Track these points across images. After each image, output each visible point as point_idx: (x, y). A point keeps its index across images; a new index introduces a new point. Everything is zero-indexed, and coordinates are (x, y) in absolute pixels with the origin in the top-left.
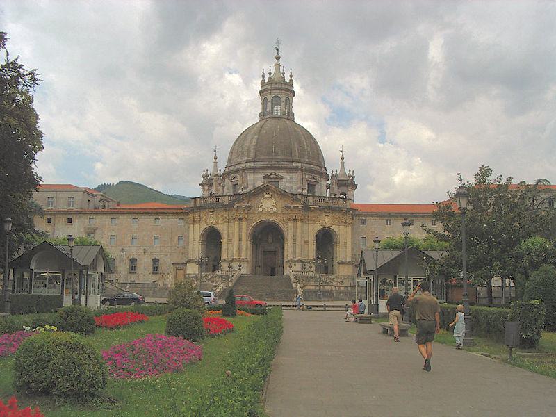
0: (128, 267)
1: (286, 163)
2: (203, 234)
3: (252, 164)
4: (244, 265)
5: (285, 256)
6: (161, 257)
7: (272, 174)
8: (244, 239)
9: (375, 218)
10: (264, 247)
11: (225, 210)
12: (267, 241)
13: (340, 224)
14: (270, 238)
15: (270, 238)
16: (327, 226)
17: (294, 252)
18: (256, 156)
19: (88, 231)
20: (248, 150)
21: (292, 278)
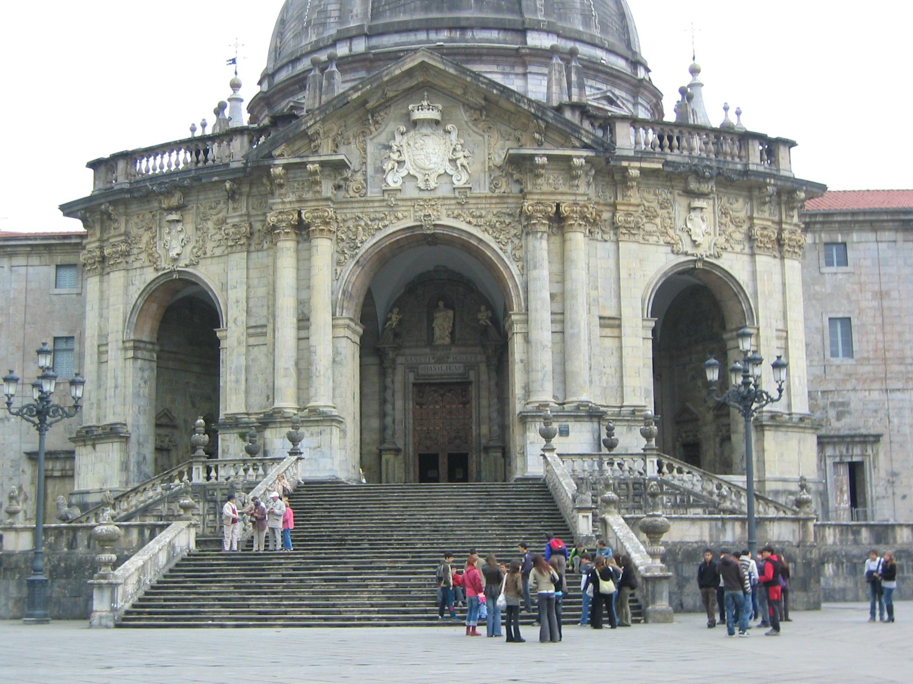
1: (494, 35)
2: (140, 311)
3: (360, 46)
5: (518, 389)
8: (322, 317)
9: (888, 235)
10: (412, 368)
11: (232, 196)
12: (430, 342)
14: (443, 323)
15: (443, 323)
16: (702, 251)
17: (563, 375)
21: (568, 487)
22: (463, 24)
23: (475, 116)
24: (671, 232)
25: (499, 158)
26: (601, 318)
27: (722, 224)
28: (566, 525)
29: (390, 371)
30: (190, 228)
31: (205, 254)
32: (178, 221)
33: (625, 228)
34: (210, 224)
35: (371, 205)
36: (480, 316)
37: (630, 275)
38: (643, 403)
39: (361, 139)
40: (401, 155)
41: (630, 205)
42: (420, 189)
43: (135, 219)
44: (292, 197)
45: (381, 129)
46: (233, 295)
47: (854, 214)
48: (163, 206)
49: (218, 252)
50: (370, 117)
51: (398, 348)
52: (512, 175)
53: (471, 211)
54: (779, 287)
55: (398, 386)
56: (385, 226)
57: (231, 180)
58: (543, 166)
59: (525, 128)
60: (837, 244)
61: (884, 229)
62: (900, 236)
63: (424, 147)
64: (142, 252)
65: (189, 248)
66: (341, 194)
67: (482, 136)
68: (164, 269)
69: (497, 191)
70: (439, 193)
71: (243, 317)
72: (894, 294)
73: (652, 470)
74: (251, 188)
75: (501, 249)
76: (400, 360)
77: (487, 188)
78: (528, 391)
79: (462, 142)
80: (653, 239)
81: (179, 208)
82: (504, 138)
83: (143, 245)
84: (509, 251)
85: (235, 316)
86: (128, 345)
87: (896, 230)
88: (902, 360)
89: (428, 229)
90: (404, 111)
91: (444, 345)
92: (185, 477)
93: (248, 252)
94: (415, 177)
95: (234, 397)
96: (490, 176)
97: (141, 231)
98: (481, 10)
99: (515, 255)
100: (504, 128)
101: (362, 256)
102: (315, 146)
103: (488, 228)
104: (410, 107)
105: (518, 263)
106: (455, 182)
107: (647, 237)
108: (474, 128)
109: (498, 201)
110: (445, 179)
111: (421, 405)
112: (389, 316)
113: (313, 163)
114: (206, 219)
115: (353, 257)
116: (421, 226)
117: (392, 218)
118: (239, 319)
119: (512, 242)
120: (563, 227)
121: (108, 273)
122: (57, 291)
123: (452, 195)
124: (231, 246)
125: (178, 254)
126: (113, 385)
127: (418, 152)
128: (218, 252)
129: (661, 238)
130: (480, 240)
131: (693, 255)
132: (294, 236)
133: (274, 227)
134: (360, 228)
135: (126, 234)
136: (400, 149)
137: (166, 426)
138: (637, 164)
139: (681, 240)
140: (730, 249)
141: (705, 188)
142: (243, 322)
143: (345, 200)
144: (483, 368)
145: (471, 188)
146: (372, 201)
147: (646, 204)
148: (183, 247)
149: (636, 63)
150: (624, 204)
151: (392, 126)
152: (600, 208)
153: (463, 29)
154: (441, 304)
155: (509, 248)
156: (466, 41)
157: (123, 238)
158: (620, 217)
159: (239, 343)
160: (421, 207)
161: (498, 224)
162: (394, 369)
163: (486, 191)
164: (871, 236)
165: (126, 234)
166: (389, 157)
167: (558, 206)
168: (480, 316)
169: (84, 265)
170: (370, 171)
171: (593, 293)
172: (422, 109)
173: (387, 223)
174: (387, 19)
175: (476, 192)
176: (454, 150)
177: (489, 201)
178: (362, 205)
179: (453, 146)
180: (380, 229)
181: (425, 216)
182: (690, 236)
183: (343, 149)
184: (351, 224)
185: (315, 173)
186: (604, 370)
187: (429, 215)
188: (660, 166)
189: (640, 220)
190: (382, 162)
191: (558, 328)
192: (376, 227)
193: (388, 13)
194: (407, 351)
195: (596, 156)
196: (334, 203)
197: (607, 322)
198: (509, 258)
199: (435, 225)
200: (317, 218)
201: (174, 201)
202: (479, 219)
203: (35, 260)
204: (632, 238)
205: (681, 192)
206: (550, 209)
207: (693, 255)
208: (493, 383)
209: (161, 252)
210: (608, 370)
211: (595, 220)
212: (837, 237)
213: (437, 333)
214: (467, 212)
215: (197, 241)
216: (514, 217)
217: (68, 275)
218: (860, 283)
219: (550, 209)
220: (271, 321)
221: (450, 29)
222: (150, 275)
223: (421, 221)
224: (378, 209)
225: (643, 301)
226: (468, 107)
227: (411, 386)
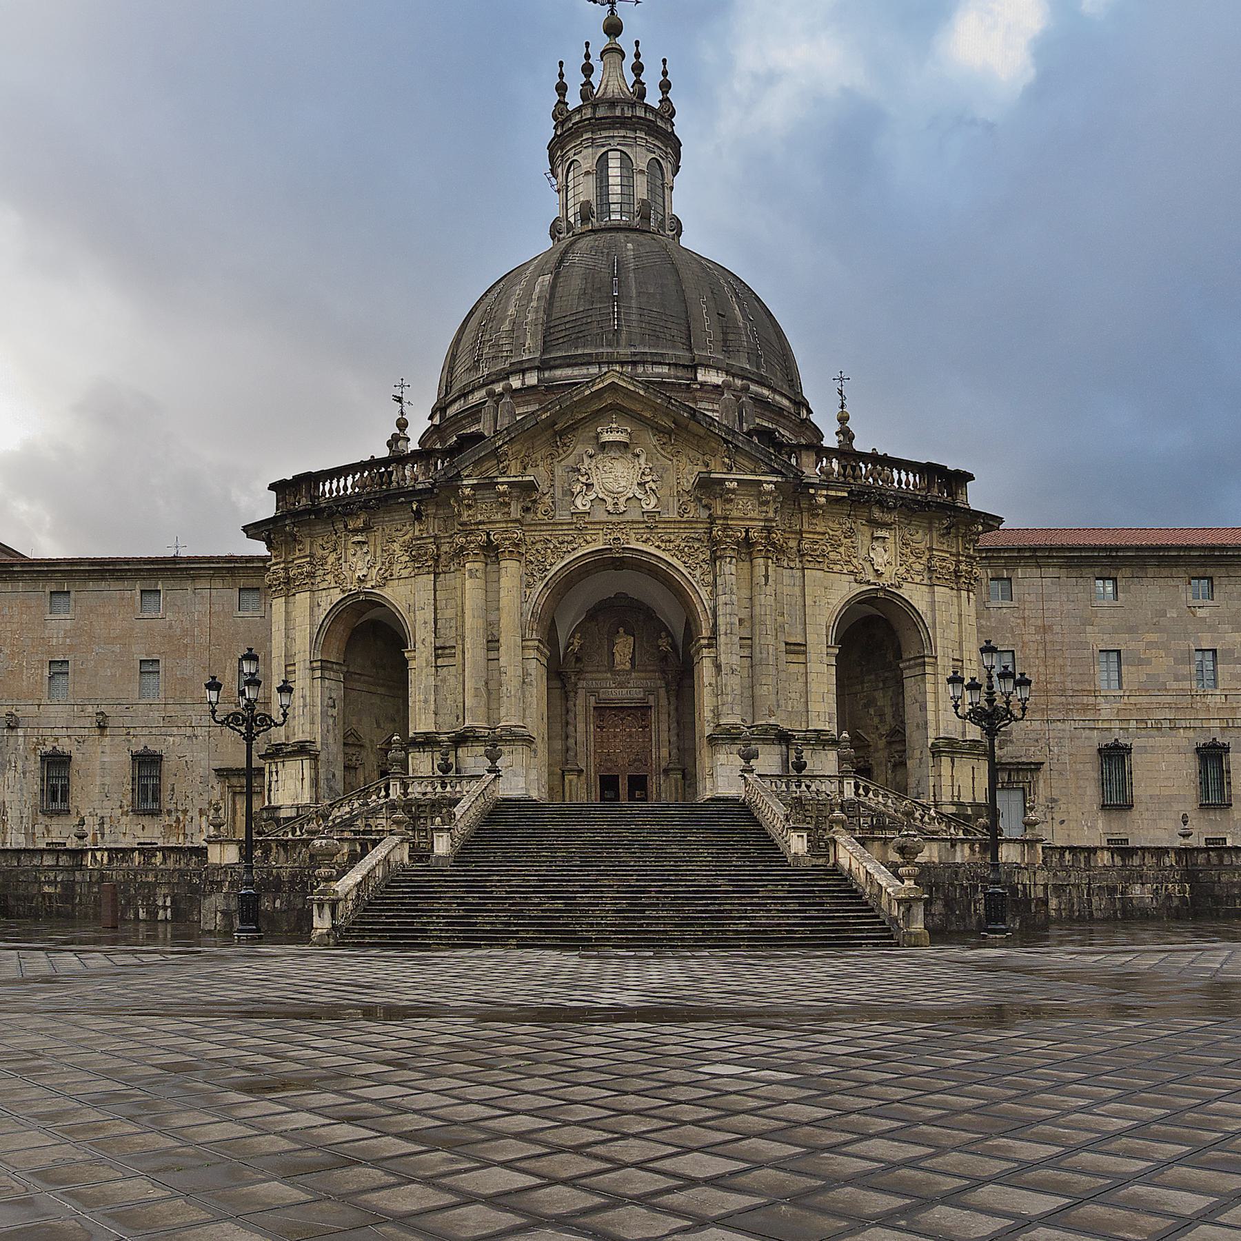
0: (37, 788)
4: (510, 759)
6: (171, 746)
8: (509, 639)
9: (1051, 572)
10: (592, 692)
12: (611, 667)
13: (933, 575)
14: (623, 648)
15: (623, 648)
16: (882, 581)
23: (665, 440)
24: (854, 561)
25: (688, 482)
26: (787, 644)
27: (903, 555)
28: (776, 845)
29: (572, 694)
31: (391, 575)
32: (364, 543)
33: (811, 555)
34: (396, 546)
35: (560, 527)
36: (660, 642)
37: (815, 602)
38: (828, 729)
39: (549, 461)
40: (589, 478)
41: (814, 533)
42: (609, 513)
45: (568, 452)
47: (1019, 550)
49: (405, 573)
50: (558, 439)
51: (581, 672)
52: (700, 500)
53: (660, 535)
54: (955, 619)
55: (580, 709)
56: (574, 549)
58: (733, 491)
60: (1003, 579)
61: (1049, 566)
62: (1063, 573)
63: (613, 470)
64: (328, 573)
65: (375, 571)
66: (529, 516)
67: (671, 460)
68: (350, 590)
69: (686, 515)
70: (627, 517)
72: (1057, 628)
73: (849, 792)
74: (436, 510)
75: (690, 574)
76: (582, 684)
77: (676, 513)
79: (651, 465)
80: (837, 568)
81: (367, 528)
82: (692, 462)
83: (328, 567)
84: (698, 576)
85: (422, 638)
86: (315, 664)
87: (1060, 567)
88: (1062, 692)
89: (617, 552)
90: (593, 434)
91: (624, 670)
92: (383, 793)
93: (436, 574)
94: (603, 500)
96: (679, 500)
99: (703, 580)
100: (692, 453)
101: (550, 579)
102: (504, 467)
103: (677, 553)
104: (599, 430)
105: (707, 588)
106: (644, 506)
107: (831, 566)
108: (662, 452)
109: (687, 526)
110: (634, 503)
111: (601, 728)
112: (571, 641)
113: (502, 484)
115: (542, 579)
116: (611, 549)
117: (582, 540)
118: (428, 640)
119: (701, 566)
120: (752, 552)
121: (294, 595)
122: (241, 614)
123: (642, 519)
124: (419, 568)
125: (363, 576)
127: (607, 475)
128: (405, 573)
129: (845, 567)
130: (670, 564)
131: (875, 584)
132: (482, 557)
133: (462, 548)
134: (549, 551)
135: (312, 556)
136: (589, 472)
137: (353, 745)
138: (825, 492)
139: (863, 569)
140: (910, 580)
141: (888, 518)
142: (431, 643)
143: (534, 522)
144: (662, 692)
145: (659, 512)
146: (561, 524)
147: (831, 533)
148: (369, 568)
149: (802, 404)
150: (810, 532)
151: (580, 449)
152: (787, 535)
154: (621, 630)
155: (698, 573)
157: (308, 559)
158: (806, 545)
160: (609, 531)
161: (686, 549)
162: (576, 693)
163: (675, 516)
164: (1036, 572)
165: (312, 556)
166: (578, 479)
167: (747, 531)
168: (660, 642)
169: (270, 587)
170: (558, 494)
171: (780, 619)
172: (611, 432)
173: (576, 546)
175: (665, 516)
176: (643, 473)
177: (677, 525)
178: (550, 528)
179: (642, 470)
180: (569, 551)
181: (614, 539)
182: (873, 565)
183: (530, 470)
184: (539, 546)
185: (503, 494)
186: (789, 695)
187: (619, 539)
188: (846, 495)
189: (825, 547)
190: (570, 485)
191: (746, 652)
192: (565, 550)
194: (588, 676)
195: (786, 482)
196: (522, 525)
197: (792, 647)
198: (698, 582)
199: (623, 549)
200: (507, 539)
201: (360, 523)
202: (668, 544)
203: (218, 583)
204: (817, 566)
205: (864, 522)
206: (739, 534)
207: (875, 584)
208: (672, 708)
209: (348, 574)
210: (793, 695)
211: (782, 546)
212: (1003, 572)
213: (618, 658)
214: (656, 537)
215: (383, 563)
216: (703, 542)
217: (250, 597)
218: (1024, 618)
219: (739, 534)
220: (460, 642)
222: (337, 596)
223: (610, 544)
224: (566, 532)
225: (827, 628)
226: (658, 430)
227: (592, 709)
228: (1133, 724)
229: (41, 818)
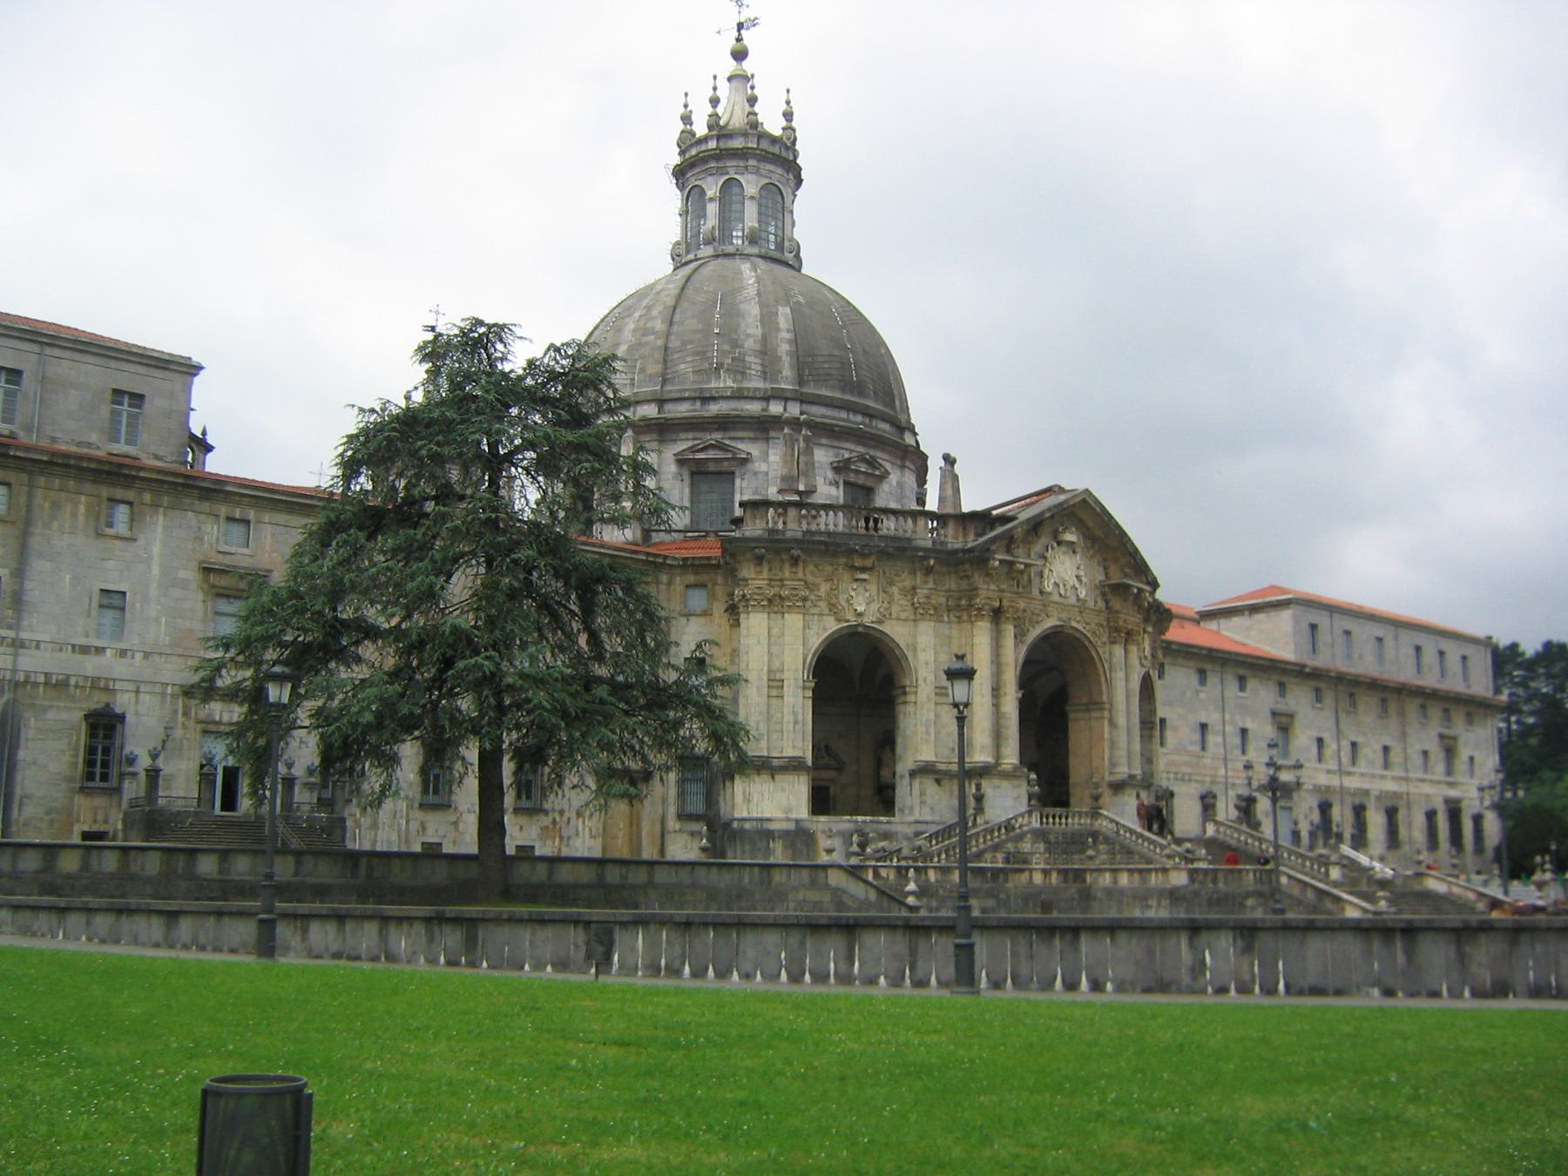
3: (794, 410)
7: (862, 459)
11: (929, 571)
18: (801, 381)
19: (223, 581)
20: (766, 350)
22: (871, 412)
30: (873, 588)
31: (890, 615)
34: (895, 590)
42: (1060, 595)
43: (811, 567)
44: (993, 587)
46: (922, 656)
48: (856, 564)
57: (935, 558)
59: (1116, 560)
65: (875, 606)
68: (848, 621)
71: (931, 678)
78: (1113, 765)
95: (924, 747)
97: (818, 580)
98: (876, 401)
113: (1021, 563)
114: (891, 583)
118: (929, 678)
126: (792, 720)
128: (903, 615)
153: (871, 416)
156: (872, 428)
159: (929, 699)
174: (810, 389)
193: (812, 384)
221: (864, 414)
222: (831, 626)
228: (1172, 776)
229: (417, 814)
